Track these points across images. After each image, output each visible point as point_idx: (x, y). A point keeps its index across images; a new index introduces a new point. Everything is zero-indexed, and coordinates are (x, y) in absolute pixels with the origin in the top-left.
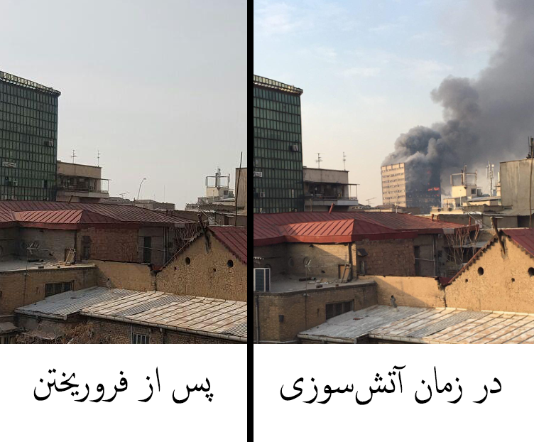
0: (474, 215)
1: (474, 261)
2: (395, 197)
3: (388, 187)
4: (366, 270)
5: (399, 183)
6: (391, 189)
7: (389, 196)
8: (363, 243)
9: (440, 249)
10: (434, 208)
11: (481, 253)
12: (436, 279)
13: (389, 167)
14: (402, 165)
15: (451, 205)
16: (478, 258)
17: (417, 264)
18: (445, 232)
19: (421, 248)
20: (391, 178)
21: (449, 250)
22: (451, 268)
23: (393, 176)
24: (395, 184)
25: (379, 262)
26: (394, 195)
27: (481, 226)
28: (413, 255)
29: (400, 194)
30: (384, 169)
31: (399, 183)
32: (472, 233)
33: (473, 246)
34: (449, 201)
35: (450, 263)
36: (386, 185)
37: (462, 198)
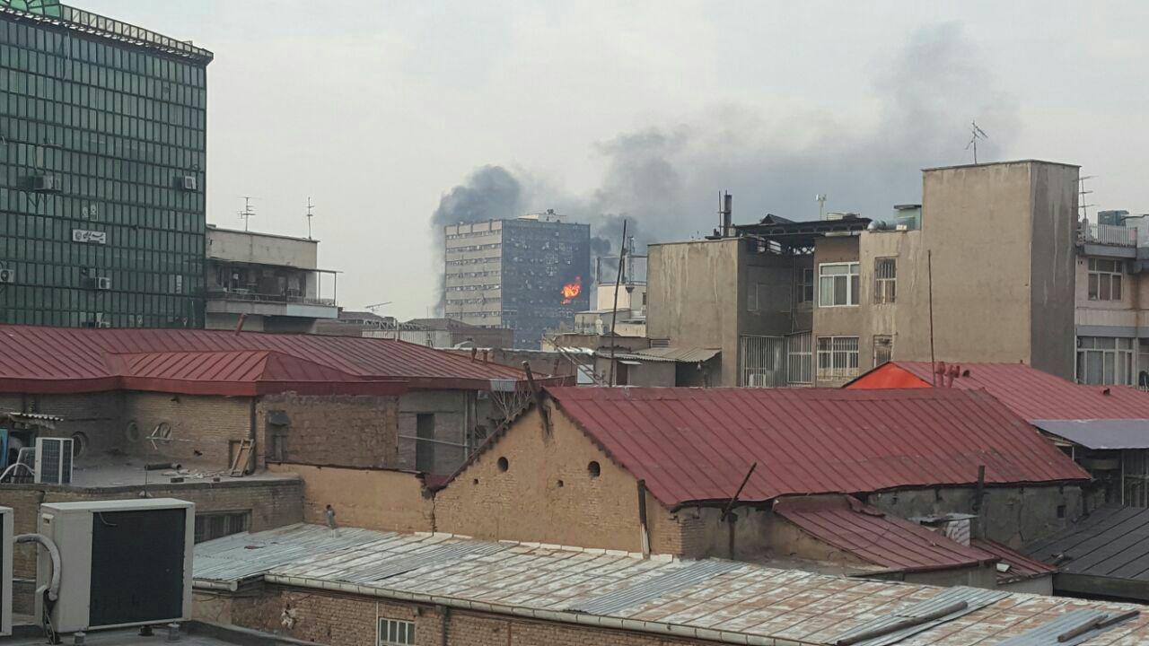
2: (476, 301)
3: (461, 276)
6: (466, 282)
7: (461, 296)
8: (282, 400)
9: (483, 422)
14: (498, 226)
20: (468, 256)
23: (474, 249)
24: (476, 268)
26: (475, 294)
29: (487, 295)
36: (456, 269)
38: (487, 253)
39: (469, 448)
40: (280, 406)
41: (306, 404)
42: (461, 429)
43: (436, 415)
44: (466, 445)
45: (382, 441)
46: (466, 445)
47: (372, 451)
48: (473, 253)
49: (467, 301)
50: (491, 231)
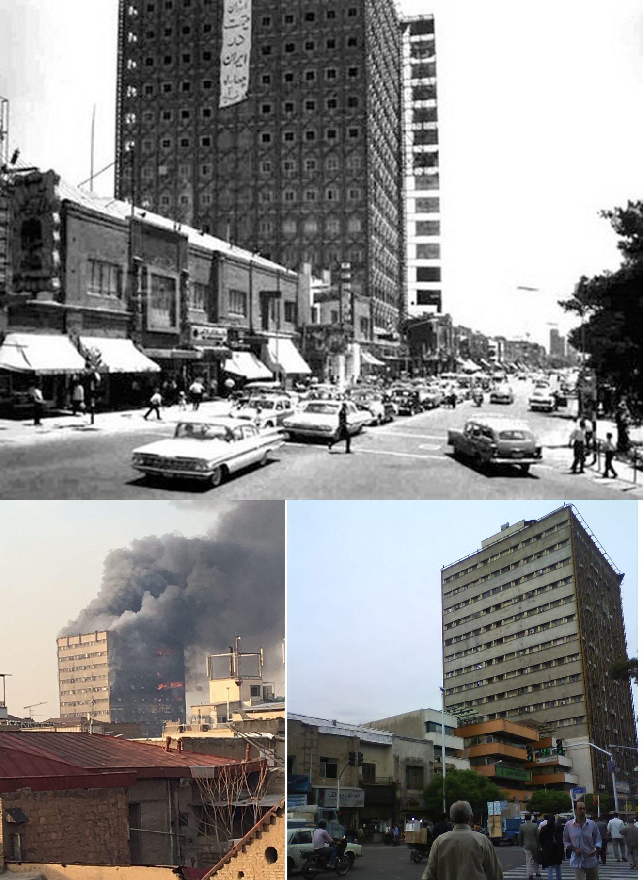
0: (258, 739)
1: (258, 835)
2: (87, 702)
3: (73, 681)
4: (24, 852)
5: (95, 672)
6: (78, 686)
7: (74, 699)
8: (17, 797)
9: (184, 809)
10: (170, 724)
11: (272, 817)
12: (174, 872)
13: (75, 640)
14: (103, 636)
15: (208, 719)
16: (265, 827)
17: (135, 838)
18: (195, 774)
19: (143, 806)
20: (77, 663)
21: (203, 811)
22: (207, 849)
23: (82, 657)
24: (85, 674)
25: (54, 836)
26: (86, 696)
27: (271, 763)
28: (126, 820)
29: (96, 696)
30: (64, 643)
31: (95, 672)
32: (253, 778)
33: (255, 803)
34: (204, 711)
35: (205, 839)
36: (68, 676)
37: (231, 703)
38: (96, 660)
39: (175, 836)
40: (16, 804)
41: (41, 801)
42: (166, 815)
43: (142, 805)
44: (170, 832)
45: (115, 834)
46: (170, 832)
47: (105, 844)
48: (83, 660)
49: (79, 702)
50: (97, 641)
